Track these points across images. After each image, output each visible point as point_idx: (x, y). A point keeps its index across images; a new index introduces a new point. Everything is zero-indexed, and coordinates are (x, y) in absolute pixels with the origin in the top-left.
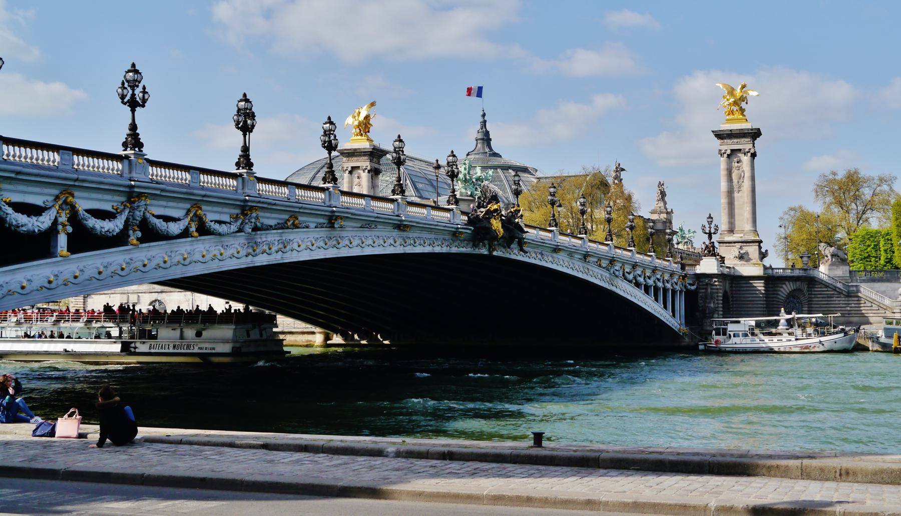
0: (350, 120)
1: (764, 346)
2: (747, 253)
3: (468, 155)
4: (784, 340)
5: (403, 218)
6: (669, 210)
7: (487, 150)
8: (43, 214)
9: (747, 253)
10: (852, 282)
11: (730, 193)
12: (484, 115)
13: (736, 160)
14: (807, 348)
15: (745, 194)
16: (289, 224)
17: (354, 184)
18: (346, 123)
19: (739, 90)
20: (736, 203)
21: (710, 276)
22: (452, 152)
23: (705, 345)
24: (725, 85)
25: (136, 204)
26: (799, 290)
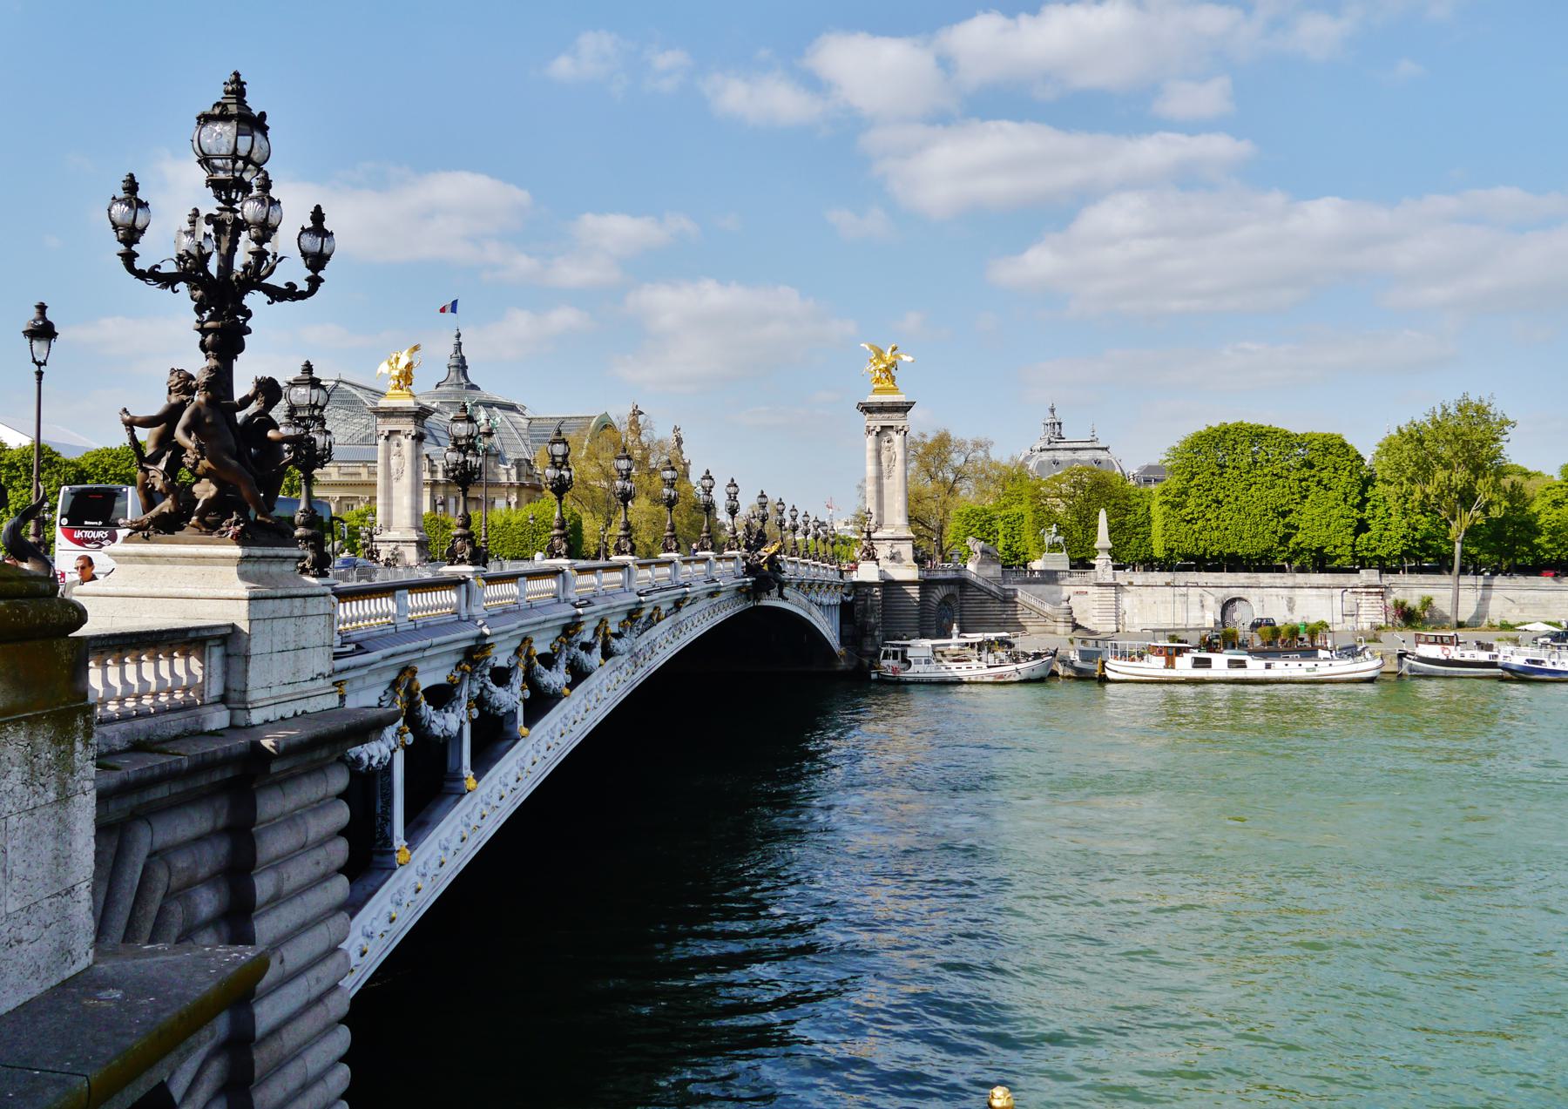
0: (384, 368)
1: (950, 675)
2: (899, 553)
3: (438, 386)
4: (974, 667)
5: (722, 584)
6: (687, 461)
7: (463, 381)
8: (512, 680)
9: (899, 553)
10: (1005, 583)
11: (879, 478)
12: (458, 336)
13: (886, 439)
14: (1001, 677)
15: (897, 481)
16: (655, 618)
17: (393, 453)
18: (379, 372)
19: (889, 354)
20: (885, 491)
21: (871, 585)
22: (708, 472)
23: (878, 673)
24: (872, 347)
25: (573, 639)
26: (951, 596)
